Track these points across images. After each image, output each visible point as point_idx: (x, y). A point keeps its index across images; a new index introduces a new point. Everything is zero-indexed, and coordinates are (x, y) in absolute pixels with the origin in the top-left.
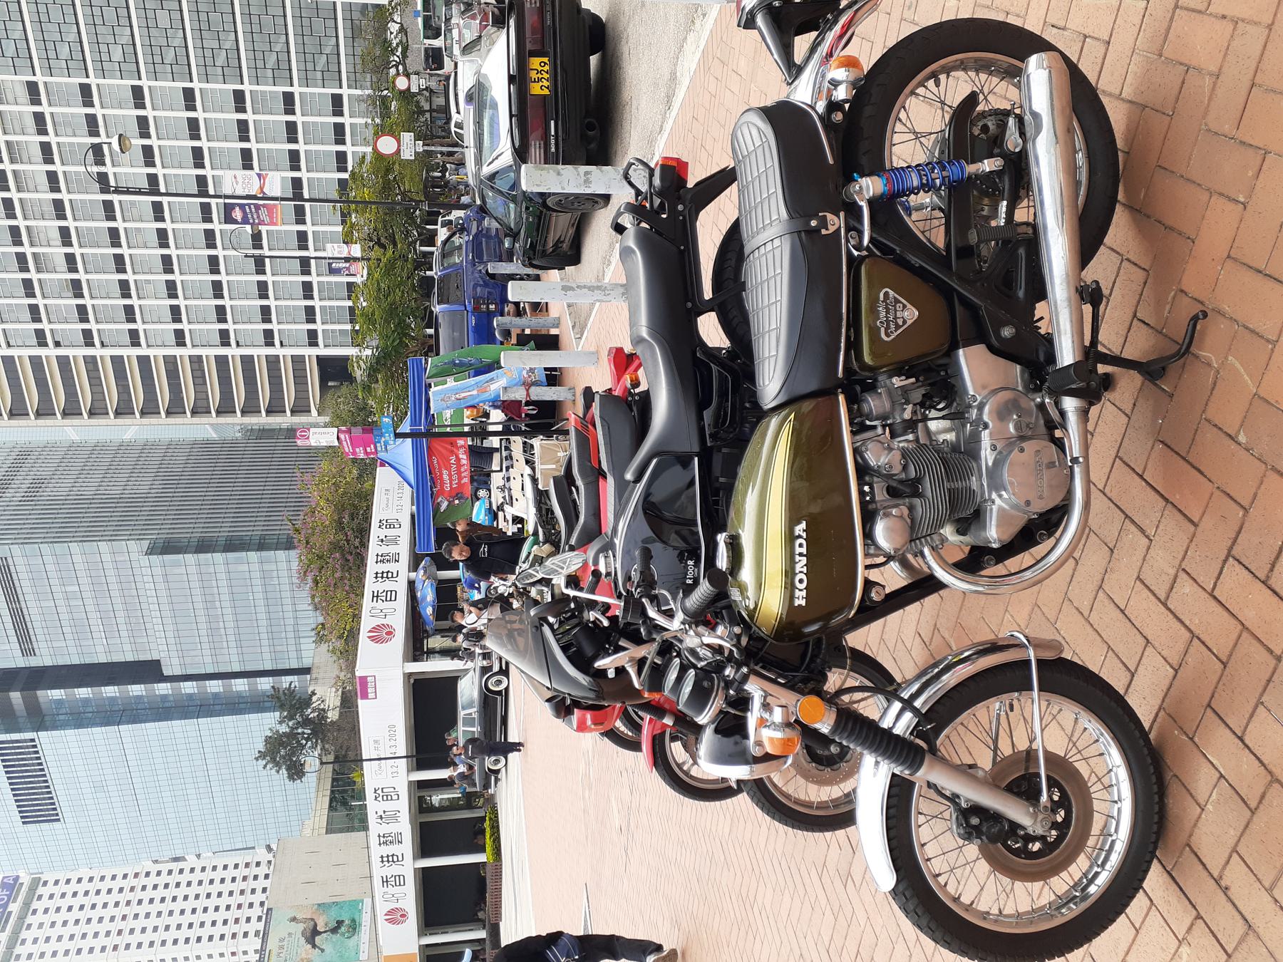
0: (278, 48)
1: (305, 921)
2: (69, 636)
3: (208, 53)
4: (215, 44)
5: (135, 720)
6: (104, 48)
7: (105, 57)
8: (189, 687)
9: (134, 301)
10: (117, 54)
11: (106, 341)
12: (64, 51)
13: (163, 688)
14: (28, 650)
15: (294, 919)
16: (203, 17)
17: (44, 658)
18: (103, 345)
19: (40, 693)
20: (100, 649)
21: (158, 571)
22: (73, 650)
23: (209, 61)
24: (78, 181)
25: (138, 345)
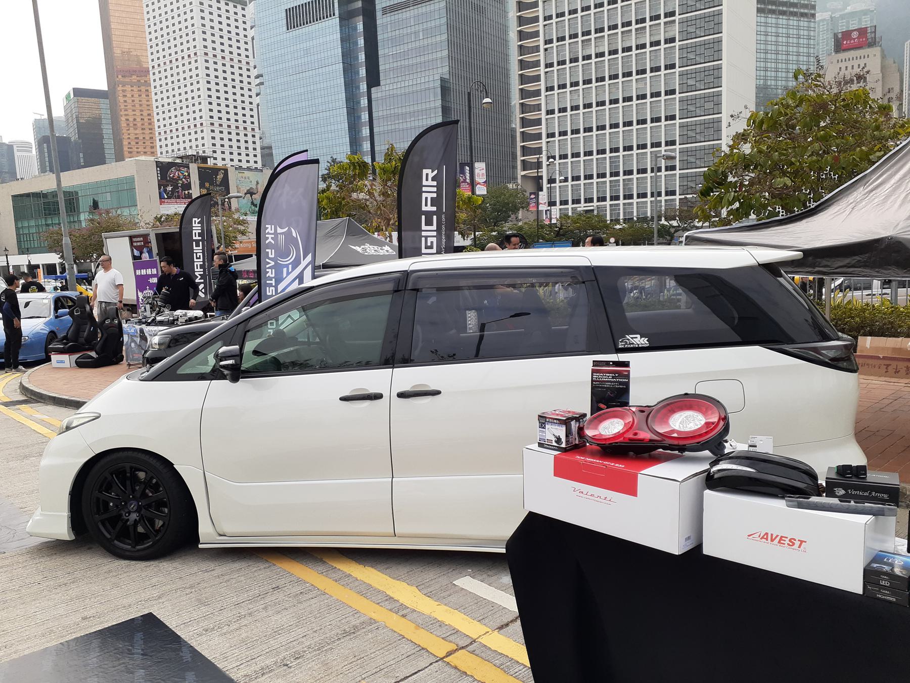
0: (698, 162)
1: (257, 188)
2: (394, 33)
3: (693, 127)
4: (698, 131)
5: (345, 71)
6: (694, 75)
7: (689, 76)
8: (364, 102)
9: (569, 89)
10: (691, 82)
11: (548, 74)
12: (692, 56)
13: (363, 87)
14: (385, 11)
15: (258, 183)
16: (711, 125)
17: (381, 20)
18: (546, 73)
19: (361, 17)
20: (386, 51)
21: (431, 85)
22: (386, 36)
23: (689, 128)
24: (628, 62)
25: (547, 91)
